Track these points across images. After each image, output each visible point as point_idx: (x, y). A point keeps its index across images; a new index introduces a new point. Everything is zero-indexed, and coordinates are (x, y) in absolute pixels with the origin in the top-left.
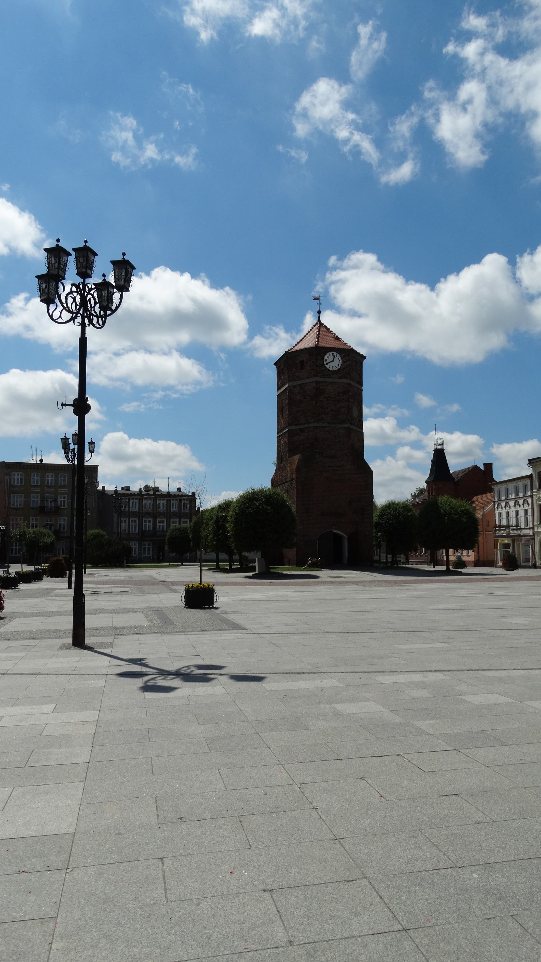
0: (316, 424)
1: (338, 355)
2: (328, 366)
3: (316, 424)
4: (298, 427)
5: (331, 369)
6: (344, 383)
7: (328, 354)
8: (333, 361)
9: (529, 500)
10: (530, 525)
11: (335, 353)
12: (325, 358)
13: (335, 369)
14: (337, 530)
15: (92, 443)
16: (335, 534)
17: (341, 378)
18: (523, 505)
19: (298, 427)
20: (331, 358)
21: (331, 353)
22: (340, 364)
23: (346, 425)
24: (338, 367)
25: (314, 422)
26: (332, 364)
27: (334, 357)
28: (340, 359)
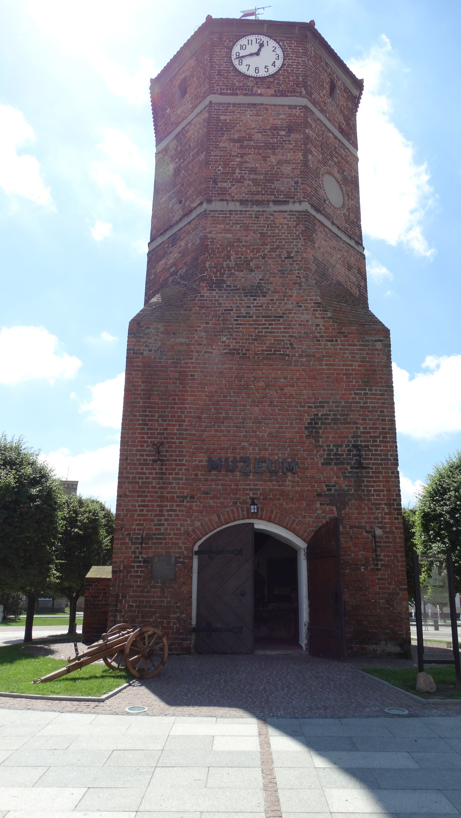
1: (272, 43)
2: (243, 69)
5: (252, 73)
6: (290, 107)
7: (243, 41)
8: (257, 54)
11: (265, 39)
12: (236, 49)
13: (262, 73)
14: (270, 520)
16: (263, 537)
17: (283, 94)
20: (254, 48)
21: (253, 38)
22: (279, 63)
23: (297, 207)
24: (272, 70)
25: (201, 203)
26: (254, 62)
27: (262, 45)
28: (279, 51)
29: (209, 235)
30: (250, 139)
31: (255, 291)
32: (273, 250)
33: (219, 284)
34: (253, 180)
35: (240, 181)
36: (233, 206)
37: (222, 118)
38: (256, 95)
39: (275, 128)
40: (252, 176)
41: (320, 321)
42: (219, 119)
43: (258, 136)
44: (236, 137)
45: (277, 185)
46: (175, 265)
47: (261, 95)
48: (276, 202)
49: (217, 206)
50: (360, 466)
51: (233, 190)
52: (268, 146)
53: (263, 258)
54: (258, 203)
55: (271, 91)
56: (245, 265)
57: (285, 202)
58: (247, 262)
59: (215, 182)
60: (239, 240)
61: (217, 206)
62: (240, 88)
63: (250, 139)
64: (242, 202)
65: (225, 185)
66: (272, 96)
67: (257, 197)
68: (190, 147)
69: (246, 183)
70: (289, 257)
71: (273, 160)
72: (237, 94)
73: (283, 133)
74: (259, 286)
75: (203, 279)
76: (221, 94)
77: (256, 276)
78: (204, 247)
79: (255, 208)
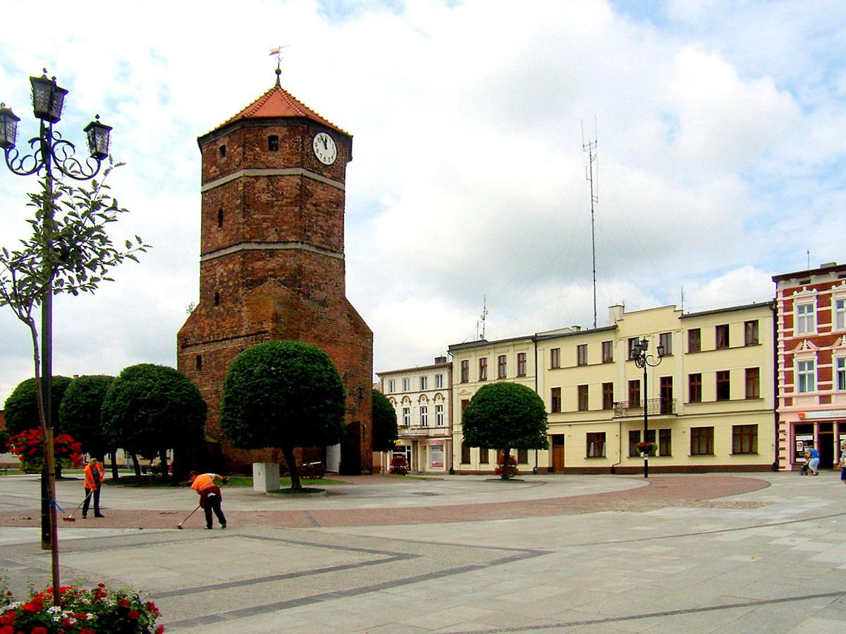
0: (299, 246)
3: (299, 246)
4: (263, 247)
9: (446, 394)
10: (446, 423)
15: (97, 131)
18: (434, 400)
19: (263, 247)
29: (303, 265)
30: (320, 206)
31: (323, 303)
32: (330, 280)
33: (307, 296)
34: (322, 234)
35: (316, 233)
36: (312, 249)
37: (308, 187)
38: (323, 175)
39: (331, 202)
40: (321, 231)
41: (349, 325)
42: (306, 188)
43: (323, 205)
44: (314, 202)
45: (331, 239)
46: (273, 271)
47: (325, 176)
48: (332, 251)
49: (305, 247)
50: (361, 397)
51: (313, 238)
52: (328, 213)
53: (326, 284)
54: (324, 249)
55: (330, 175)
56: (318, 287)
57: (335, 252)
58: (320, 285)
59: (305, 231)
60: (316, 271)
61: (305, 247)
62: (316, 169)
63: (320, 206)
64: (317, 247)
65: (310, 234)
66: (330, 179)
67: (324, 246)
68: (282, 193)
69: (319, 235)
70: (337, 286)
71: (330, 222)
72: (314, 172)
73: (334, 206)
74: (325, 301)
75: (299, 291)
76: (308, 170)
77: (324, 294)
78: (299, 270)
79: (323, 253)
